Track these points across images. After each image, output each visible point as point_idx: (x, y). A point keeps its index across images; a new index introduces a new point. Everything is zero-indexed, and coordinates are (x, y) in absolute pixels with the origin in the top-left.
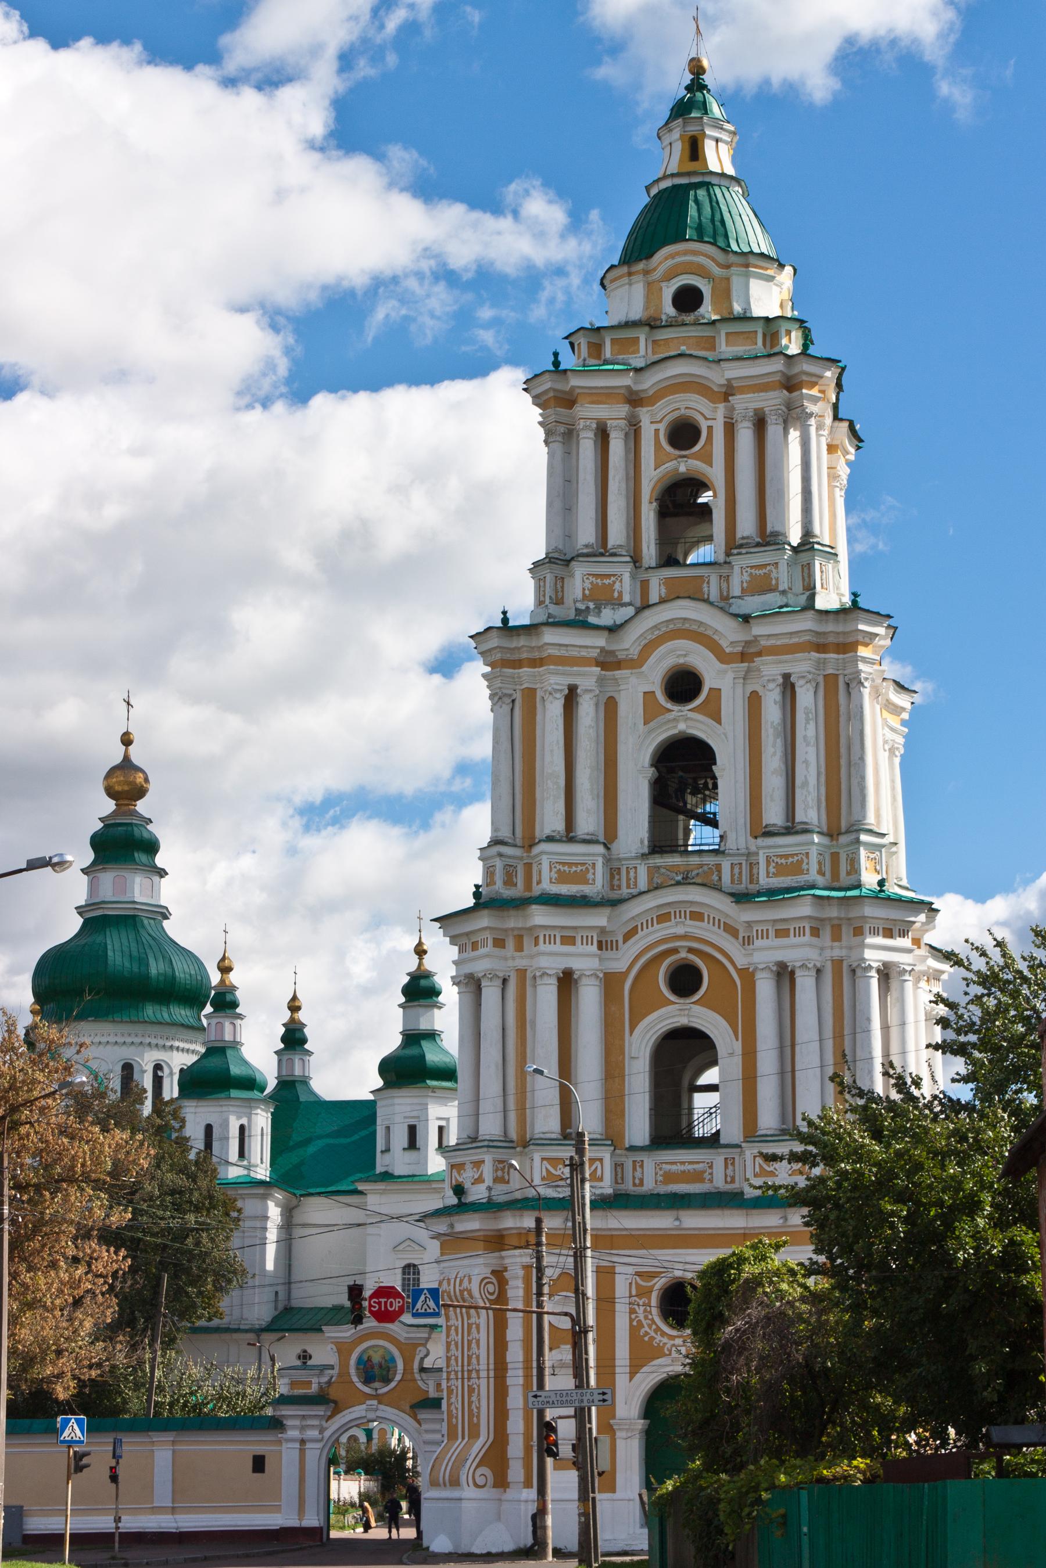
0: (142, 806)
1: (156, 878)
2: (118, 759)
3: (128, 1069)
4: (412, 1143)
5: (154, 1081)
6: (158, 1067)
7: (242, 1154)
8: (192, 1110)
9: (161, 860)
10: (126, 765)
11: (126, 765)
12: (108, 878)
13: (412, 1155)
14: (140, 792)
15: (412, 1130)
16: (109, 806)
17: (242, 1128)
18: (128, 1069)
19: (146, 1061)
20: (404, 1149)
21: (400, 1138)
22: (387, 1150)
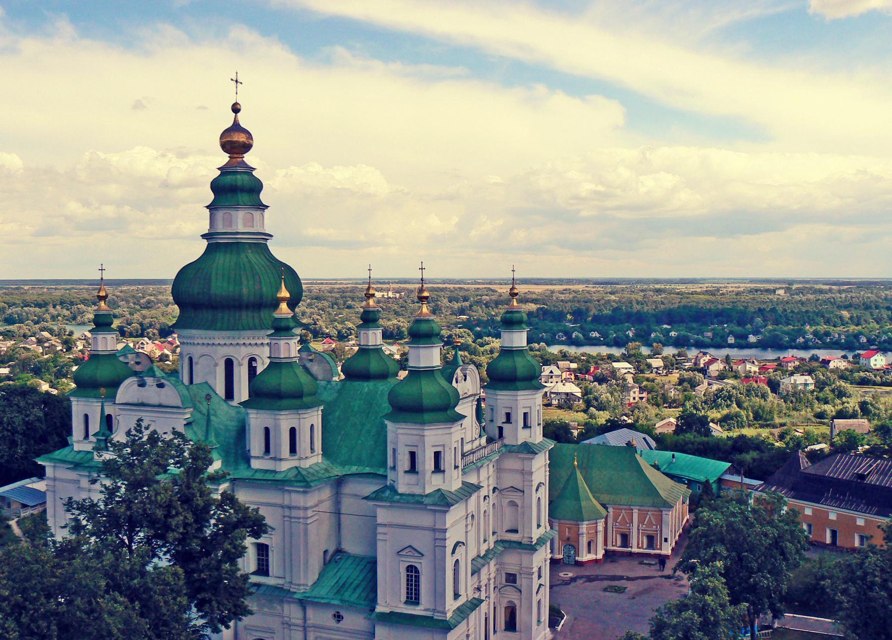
0: (249, 158)
1: (257, 214)
2: (229, 124)
3: (229, 364)
4: (413, 469)
5: (249, 370)
6: (252, 360)
7: (293, 450)
8: (254, 416)
9: (264, 197)
10: (236, 127)
11: (236, 127)
12: (220, 214)
13: (412, 478)
14: (247, 147)
15: (413, 455)
16: (224, 158)
17: (293, 431)
18: (229, 364)
19: (241, 356)
20: (406, 472)
21: (404, 463)
22: (394, 468)
